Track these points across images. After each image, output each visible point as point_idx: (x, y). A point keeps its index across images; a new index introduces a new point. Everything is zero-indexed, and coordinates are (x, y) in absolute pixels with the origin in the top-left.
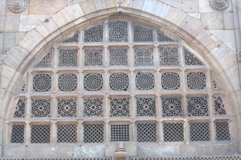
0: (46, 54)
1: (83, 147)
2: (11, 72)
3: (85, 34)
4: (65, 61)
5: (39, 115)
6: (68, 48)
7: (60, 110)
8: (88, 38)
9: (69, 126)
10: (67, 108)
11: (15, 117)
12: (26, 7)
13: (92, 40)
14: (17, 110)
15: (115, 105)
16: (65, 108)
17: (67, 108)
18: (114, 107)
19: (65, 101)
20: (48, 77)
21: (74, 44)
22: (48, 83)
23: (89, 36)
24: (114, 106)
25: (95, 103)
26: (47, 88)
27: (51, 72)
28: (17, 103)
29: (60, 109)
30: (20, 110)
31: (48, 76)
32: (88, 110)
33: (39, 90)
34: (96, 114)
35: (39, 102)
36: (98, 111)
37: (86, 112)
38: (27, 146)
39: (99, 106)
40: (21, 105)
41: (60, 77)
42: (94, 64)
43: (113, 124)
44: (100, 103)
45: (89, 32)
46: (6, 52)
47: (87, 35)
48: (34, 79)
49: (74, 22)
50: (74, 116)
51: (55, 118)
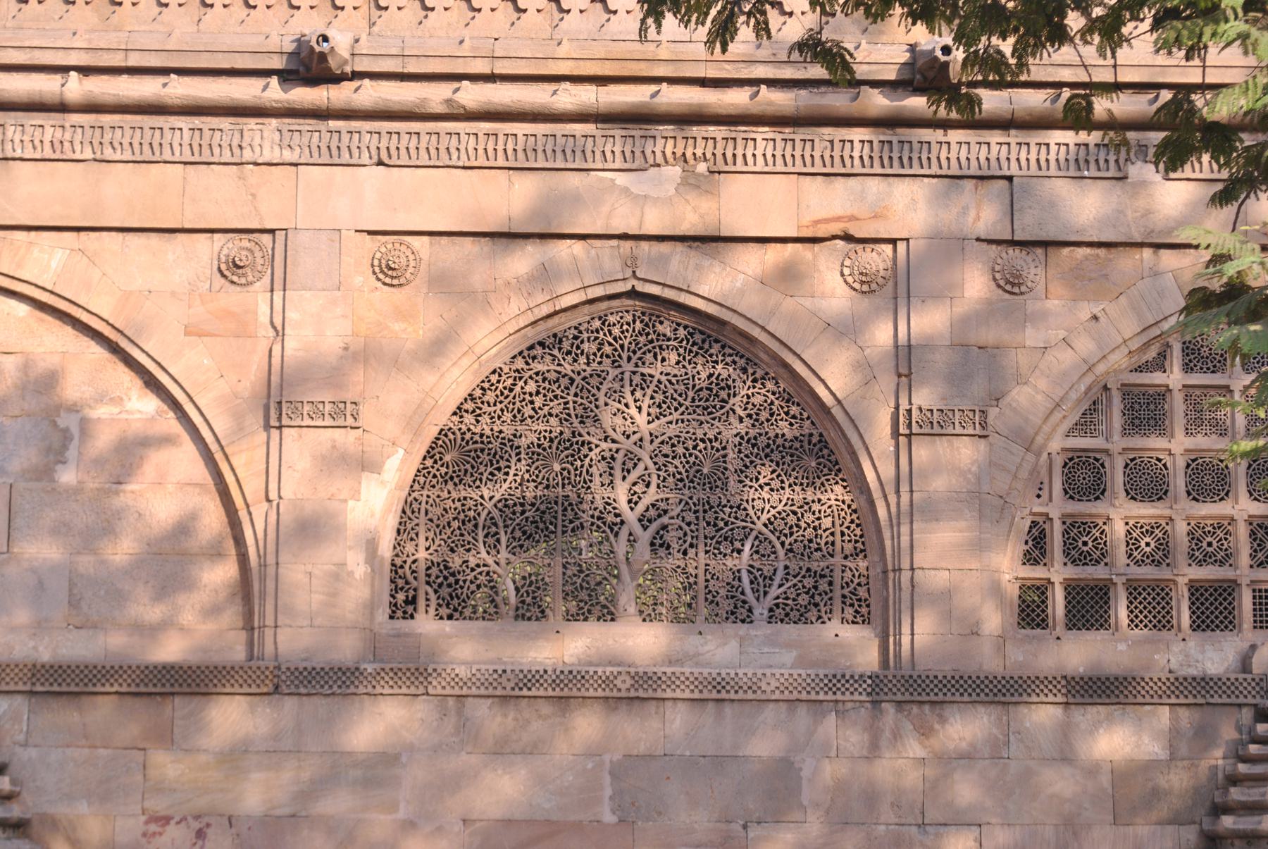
0: (1089, 403)
1: (1191, 644)
2: (1013, 454)
3: (1183, 351)
4: (1137, 422)
5: (1080, 560)
6: (1143, 389)
7: (1131, 549)
8: (1190, 361)
9: (1153, 590)
10: (1148, 544)
11: (1024, 564)
12: (1038, 277)
13: (1201, 368)
14: (1027, 547)
15: (1261, 540)
16: (1143, 544)
17: (1148, 544)
18: (1259, 545)
19: (1142, 527)
20: (1098, 464)
21: (1157, 378)
22: (1099, 479)
23: (1192, 357)
24: (1258, 542)
25: (1214, 533)
26: (1098, 493)
27: (1106, 451)
28: (1027, 529)
29: (1131, 546)
30: (1036, 548)
31: (1097, 460)
32: (1198, 549)
33: (1077, 497)
34: (1216, 561)
35: (1079, 527)
36: (1222, 554)
37: (1193, 555)
38: (1058, 638)
39: (1224, 541)
40: (1037, 534)
41: (1127, 465)
42: (1208, 432)
43: (1257, 587)
44: (1226, 534)
45: (1192, 346)
46: (998, 400)
47: (1188, 355)
48: (1064, 467)
49: (1159, 325)
50: (1164, 565)
51: (1122, 571)
